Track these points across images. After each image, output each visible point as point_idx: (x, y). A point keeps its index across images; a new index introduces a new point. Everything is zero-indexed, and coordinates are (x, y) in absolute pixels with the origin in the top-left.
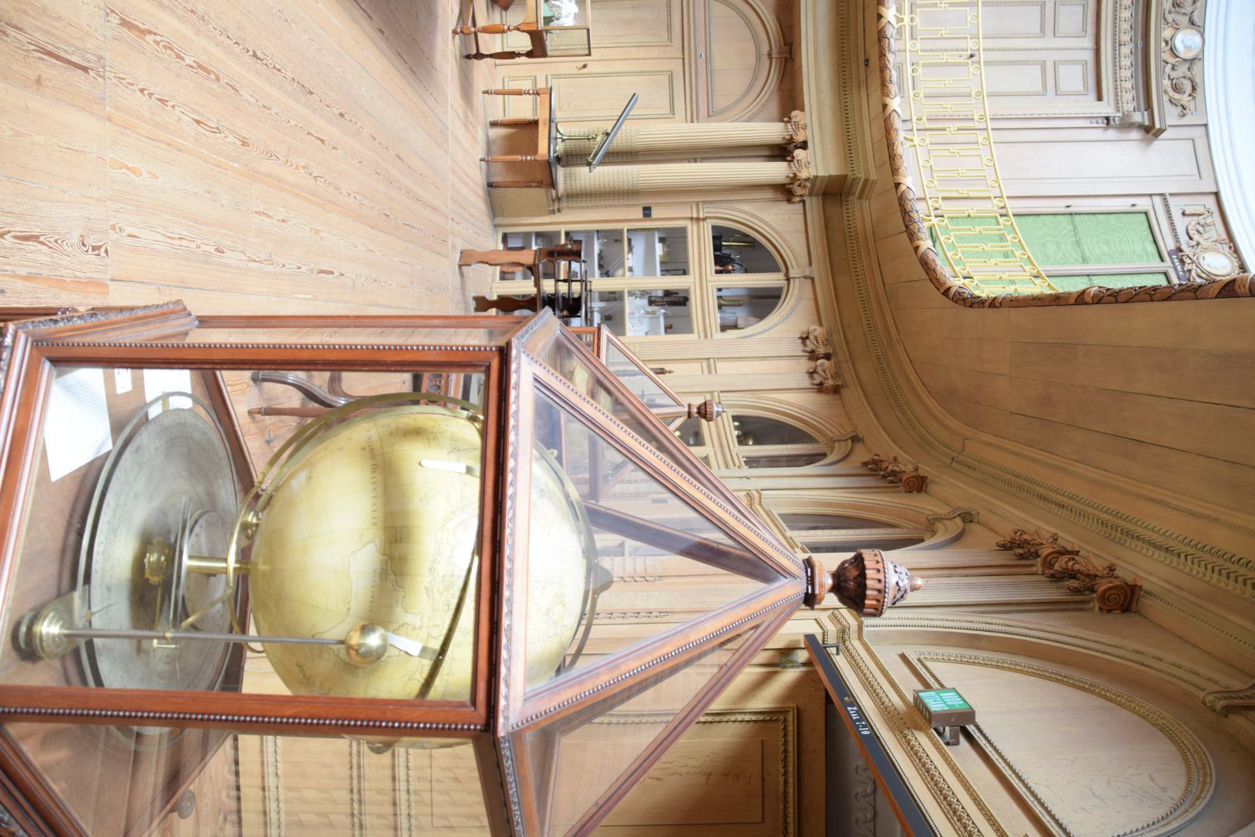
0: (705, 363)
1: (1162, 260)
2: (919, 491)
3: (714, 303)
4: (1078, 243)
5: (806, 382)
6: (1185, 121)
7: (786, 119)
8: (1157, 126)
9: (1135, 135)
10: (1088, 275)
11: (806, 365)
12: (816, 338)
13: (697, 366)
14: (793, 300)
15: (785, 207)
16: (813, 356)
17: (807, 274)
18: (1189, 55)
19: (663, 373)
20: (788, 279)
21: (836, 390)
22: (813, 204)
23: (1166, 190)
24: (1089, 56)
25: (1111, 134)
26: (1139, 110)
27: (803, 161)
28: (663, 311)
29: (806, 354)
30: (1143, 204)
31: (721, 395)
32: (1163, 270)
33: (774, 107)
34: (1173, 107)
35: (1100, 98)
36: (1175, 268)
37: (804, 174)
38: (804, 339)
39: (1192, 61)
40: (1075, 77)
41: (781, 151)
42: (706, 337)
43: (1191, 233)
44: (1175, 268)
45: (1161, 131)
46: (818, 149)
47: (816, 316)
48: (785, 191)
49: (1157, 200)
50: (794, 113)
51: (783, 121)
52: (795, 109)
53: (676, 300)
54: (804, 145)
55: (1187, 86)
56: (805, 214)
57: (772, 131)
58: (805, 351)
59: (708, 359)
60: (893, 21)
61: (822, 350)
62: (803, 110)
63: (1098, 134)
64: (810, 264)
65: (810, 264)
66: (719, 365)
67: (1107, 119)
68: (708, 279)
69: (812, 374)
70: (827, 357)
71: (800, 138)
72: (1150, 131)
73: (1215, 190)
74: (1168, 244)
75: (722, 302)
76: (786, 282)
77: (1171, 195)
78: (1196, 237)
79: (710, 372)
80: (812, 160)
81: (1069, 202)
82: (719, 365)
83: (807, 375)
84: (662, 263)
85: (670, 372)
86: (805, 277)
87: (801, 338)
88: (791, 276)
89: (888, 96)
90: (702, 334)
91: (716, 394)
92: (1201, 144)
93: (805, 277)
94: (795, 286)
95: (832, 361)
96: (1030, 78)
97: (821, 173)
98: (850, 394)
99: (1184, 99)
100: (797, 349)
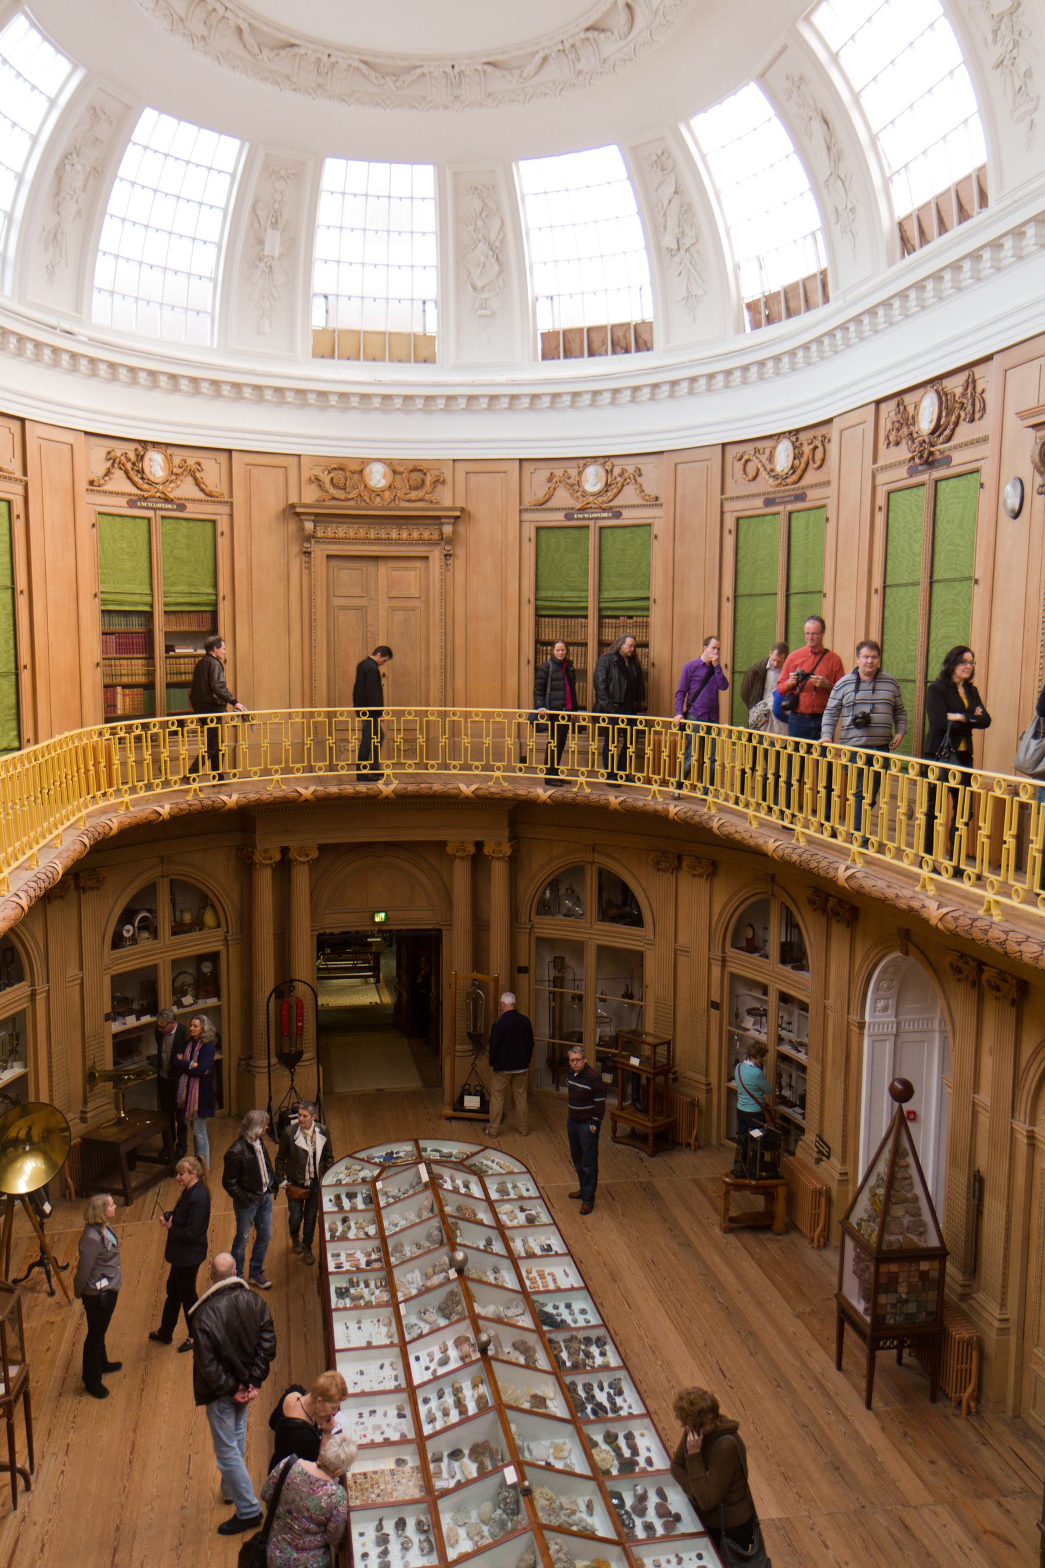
6: (449, 480)
8: (458, 513)
9: (461, 528)
18: (390, 474)
21: (714, 864)
26: (442, 524)
30: (529, 531)
32: (597, 530)
34: (437, 490)
35: (427, 558)
39: (395, 472)
41: (478, 861)
49: (527, 516)
50: (450, 849)
54: (479, 845)
60: (392, 787)
63: (459, 563)
67: (446, 555)
70: (680, 859)
71: (472, 850)
72: (461, 517)
73: (518, 462)
77: (520, 504)
81: (525, 599)
92: (470, 467)
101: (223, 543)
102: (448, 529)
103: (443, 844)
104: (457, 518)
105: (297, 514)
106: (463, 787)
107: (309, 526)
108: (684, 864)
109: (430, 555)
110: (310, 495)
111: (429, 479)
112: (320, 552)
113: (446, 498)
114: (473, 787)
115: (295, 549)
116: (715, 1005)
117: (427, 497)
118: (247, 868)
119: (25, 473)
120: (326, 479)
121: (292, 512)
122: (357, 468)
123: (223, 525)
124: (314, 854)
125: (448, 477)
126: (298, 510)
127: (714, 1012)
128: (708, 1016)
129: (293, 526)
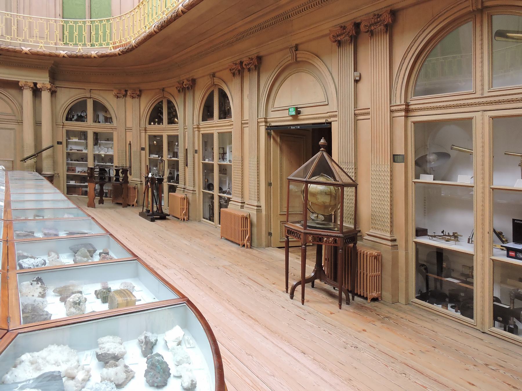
0: (127, 131)
2: (195, 81)
3: (97, 124)
5: (137, 100)
7: (22, 88)
11: (129, 99)
12: (117, 93)
13: (128, 133)
14: (100, 98)
15: (58, 93)
16: (125, 96)
17: (89, 91)
19: (131, 144)
20: (90, 98)
21: (140, 91)
22: (58, 84)
27: (43, 85)
28: (99, 141)
29: (124, 97)
31: (141, 127)
33: (13, 92)
37: (49, 86)
38: (118, 97)
41: (36, 92)
42: (116, 129)
46: (37, 79)
47: (107, 91)
48: (53, 93)
50: (20, 84)
51: (23, 90)
52: (18, 84)
53: (97, 136)
54: (35, 84)
56: (62, 87)
57: (28, 94)
58: (123, 98)
59: (125, 129)
61: (124, 93)
62: (18, 82)
64: (85, 89)
65: (85, 89)
66: (127, 126)
68: (89, 124)
69: (133, 97)
70: (126, 91)
71: (32, 85)
75: (97, 121)
76: (91, 99)
79: (131, 129)
80: (42, 82)
82: (127, 126)
83: (133, 99)
84: (79, 140)
85: (130, 142)
86: (90, 92)
87: (117, 98)
88: (89, 97)
89: (21, 51)
90: (114, 130)
91: (140, 129)
93: (90, 92)
94: (93, 96)
95: (128, 90)
97: (48, 80)
98: (142, 86)
100: (122, 100)
106: (23, 48)
108: (128, 94)
114: (29, 49)
116: (143, 149)
127: (143, 152)
128: (140, 154)
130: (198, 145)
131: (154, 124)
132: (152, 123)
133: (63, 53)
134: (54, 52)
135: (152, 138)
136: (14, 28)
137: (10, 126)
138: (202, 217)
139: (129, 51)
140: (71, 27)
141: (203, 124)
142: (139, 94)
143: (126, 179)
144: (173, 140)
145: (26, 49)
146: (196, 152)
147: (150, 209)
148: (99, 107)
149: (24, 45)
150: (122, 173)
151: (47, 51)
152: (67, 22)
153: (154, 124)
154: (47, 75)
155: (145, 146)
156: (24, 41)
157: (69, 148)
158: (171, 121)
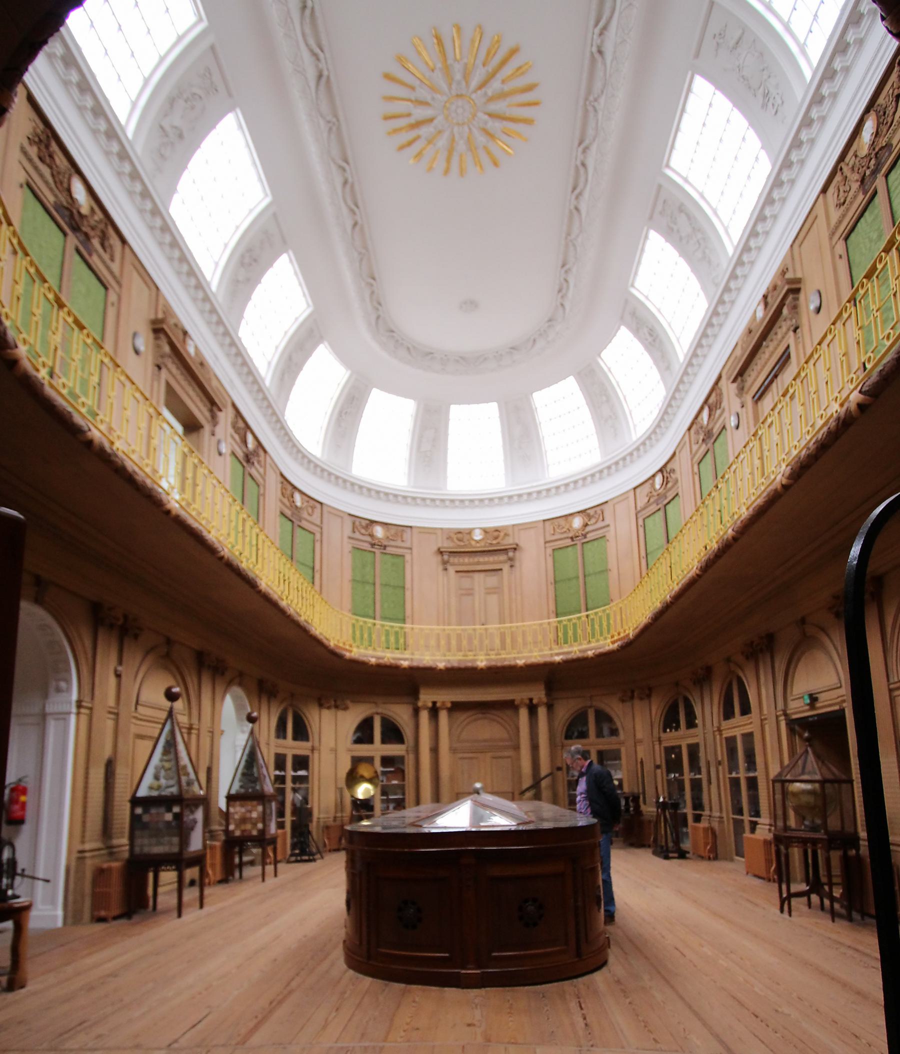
1: (576, 544)
4: (569, 579)
9: (517, 553)
10: (585, 576)
11: (637, 702)
16: (632, 698)
18: (483, 533)
21: (650, 689)
23: (542, 541)
24: (482, 575)
25: (517, 564)
30: (549, 551)
33: (509, 712)
35: (501, 570)
36: (580, 540)
40: (492, 580)
41: (532, 709)
43: (562, 531)
44: (580, 540)
45: (517, 545)
49: (547, 545)
54: (531, 700)
55: (496, 534)
57: (524, 713)
69: (641, 699)
70: (633, 692)
73: (542, 523)
74: (568, 542)
77: (545, 538)
78: (565, 530)
96: (493, 599)
99: (502, 534)
100: (629, 704)
101: (408, 567)
102: (511, 554)
103: (512, 701)
104: (515, 549)
105: (441, 553)
107: (446, 557)
108: (636, 694)
109: (504, 569)
110: (448, 545)
111: (502, 534)
112: (451, 570)
113: (509, 542)
115: (441, 567)
117: (501, 542)
118: (416, 711)
119: (322, 523)
120: (455, 537)
121: (440, 552)
122: (467, 532)
123: (408, 557)
124: (449, 705)
125: (510, 532)
126: (442, 550)
129: (439, 558)
130: (722, 753)
131: (671, 731)
132: (668, 730)
133: (558, 659)
134: (548, 659)
135: (669, 750)
136: (508, 640)
137: (506, 754)
138: (734, 853)
139: (628, 646)
140: (565, 627)
141: (725, 724)
142: (647, 694)
143: (637, 807)
144: (694, 750)
145: (520, 662)
146: (719, 763)
147: (663, 844)
148: (603, 718)
149: (519, 658)
150: (632, 801)
151: (541, 660)
152: (559, 622)
153: (671, 731)
154: (542, 687)
155: (661, 762)
156: (518, 653)
157: (570, 775)
158: (691, 724)
